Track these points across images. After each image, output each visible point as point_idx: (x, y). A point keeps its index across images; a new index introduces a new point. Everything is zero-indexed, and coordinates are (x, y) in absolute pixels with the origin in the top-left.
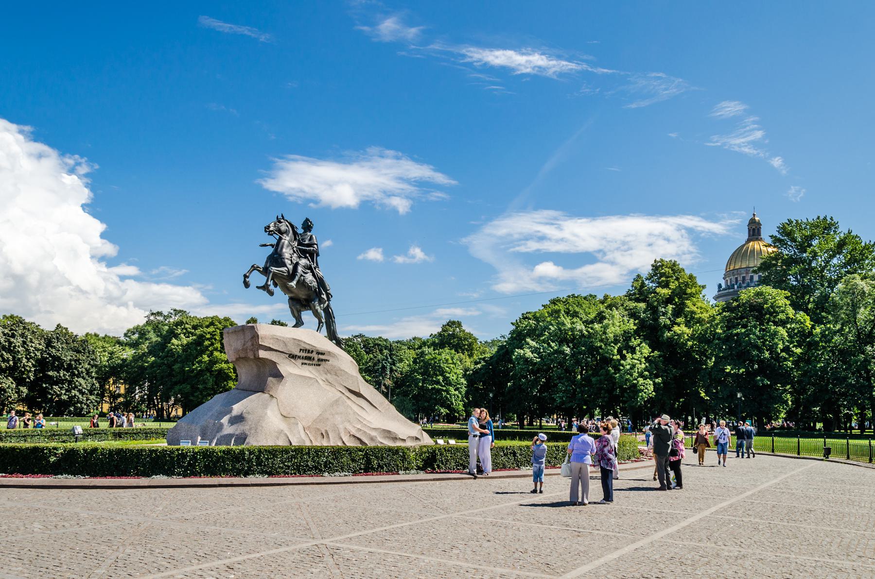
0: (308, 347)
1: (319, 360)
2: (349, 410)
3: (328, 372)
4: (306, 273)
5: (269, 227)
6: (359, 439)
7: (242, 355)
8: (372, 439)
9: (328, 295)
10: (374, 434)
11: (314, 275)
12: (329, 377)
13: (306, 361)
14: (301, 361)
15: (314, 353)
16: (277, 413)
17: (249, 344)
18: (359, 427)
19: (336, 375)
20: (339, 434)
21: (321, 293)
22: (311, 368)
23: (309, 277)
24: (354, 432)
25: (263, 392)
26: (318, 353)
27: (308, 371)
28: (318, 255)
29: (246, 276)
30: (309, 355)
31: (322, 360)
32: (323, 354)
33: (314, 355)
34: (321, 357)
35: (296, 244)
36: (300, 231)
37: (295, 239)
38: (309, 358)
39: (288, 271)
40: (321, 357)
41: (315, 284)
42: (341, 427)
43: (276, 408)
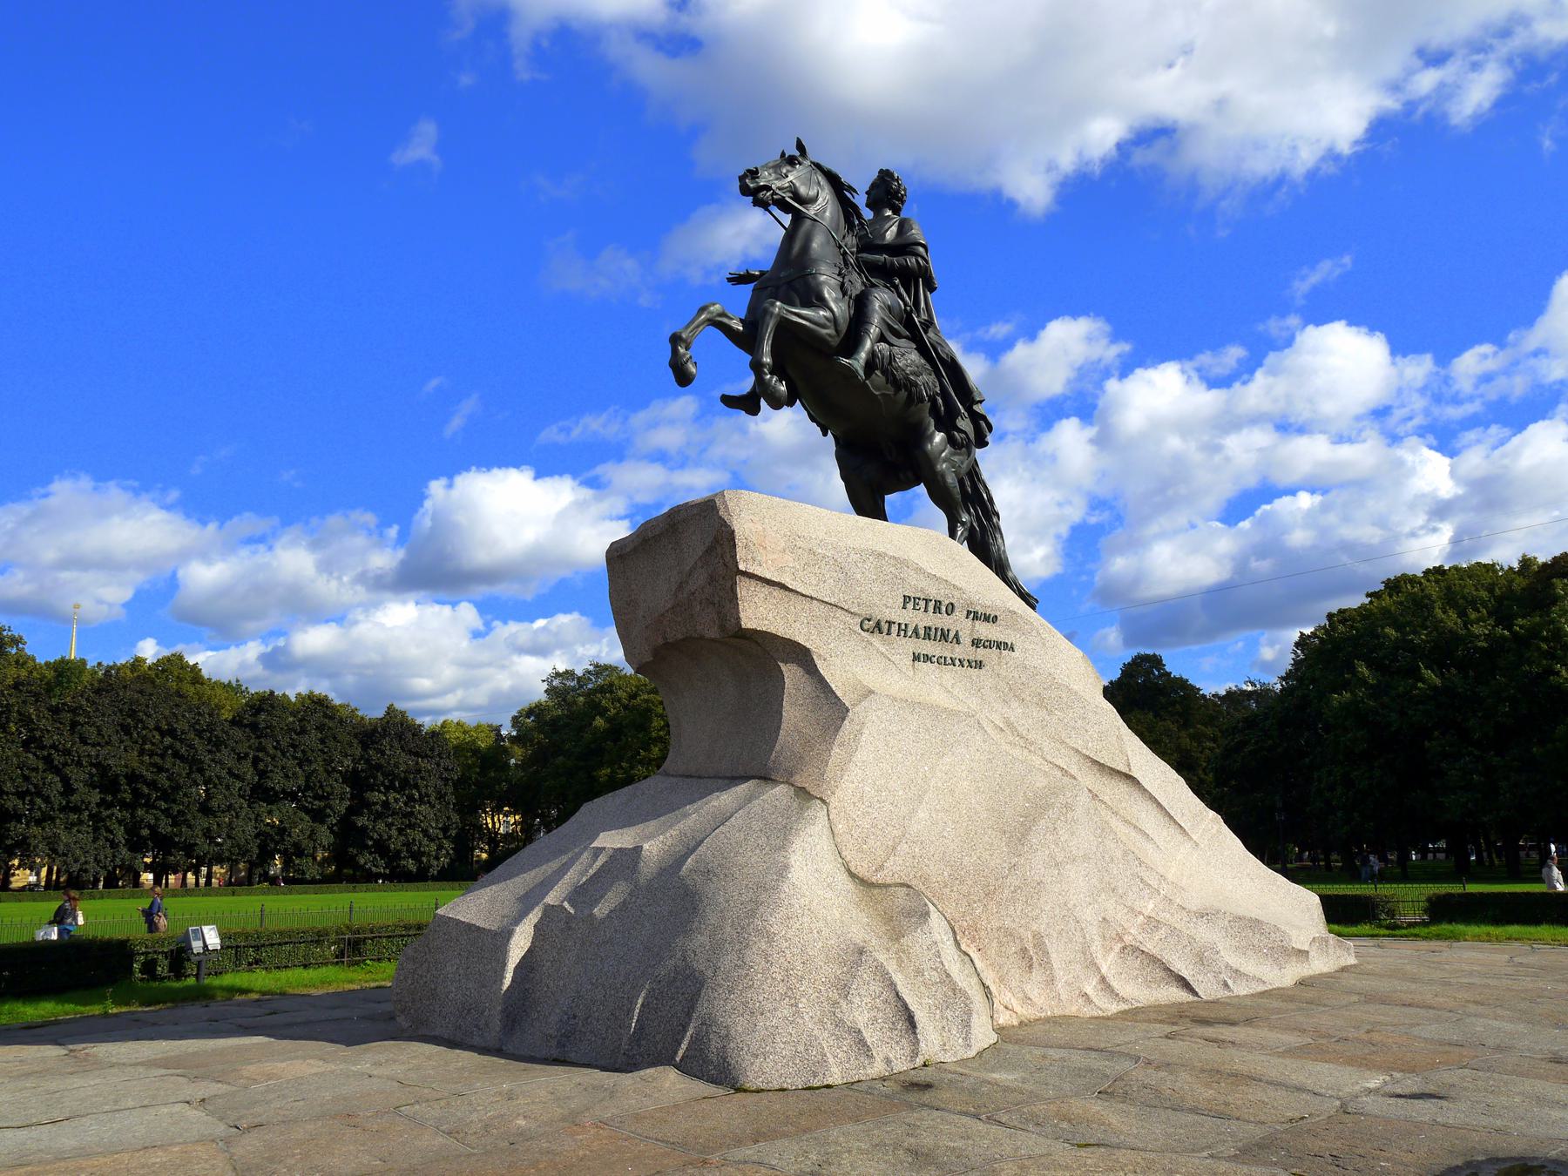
0: (934, 592)
1: (976, 643)
2: (1110, 844)
3: (1013, 693)
4: (898, 335)
5: (754, 174)
6: (1154, 960)
7: (676, 634)
8: (1202, 958)
9: (977, 418)
10: (1205, 934)
11: (923, 349)
12: (1015, 711)
13: (928, 647)
15: (959, 614)
16: (830, 866)
17: (700, 578)
18: (1149, 907)
19: (1041, 703)
20: (1085, 950)
21: (952, 414)
22: (949, 675)
23: (908, 358)
24: (1134, 934)
25: (766, 778)
26: (975, 616)
28: (930, 287)
29: (675, 340)
30: (941, 621)
31: (989, 644)
32: (990, 619)
33: (957, 622)
34: (984, 631)
35: (851, 241)
37: (851, 226)
38: (944, 636)
39: (835, 320)
40: (984, 631)
41: (927, 381)
42: (1089, 915)
43: (824, 844)
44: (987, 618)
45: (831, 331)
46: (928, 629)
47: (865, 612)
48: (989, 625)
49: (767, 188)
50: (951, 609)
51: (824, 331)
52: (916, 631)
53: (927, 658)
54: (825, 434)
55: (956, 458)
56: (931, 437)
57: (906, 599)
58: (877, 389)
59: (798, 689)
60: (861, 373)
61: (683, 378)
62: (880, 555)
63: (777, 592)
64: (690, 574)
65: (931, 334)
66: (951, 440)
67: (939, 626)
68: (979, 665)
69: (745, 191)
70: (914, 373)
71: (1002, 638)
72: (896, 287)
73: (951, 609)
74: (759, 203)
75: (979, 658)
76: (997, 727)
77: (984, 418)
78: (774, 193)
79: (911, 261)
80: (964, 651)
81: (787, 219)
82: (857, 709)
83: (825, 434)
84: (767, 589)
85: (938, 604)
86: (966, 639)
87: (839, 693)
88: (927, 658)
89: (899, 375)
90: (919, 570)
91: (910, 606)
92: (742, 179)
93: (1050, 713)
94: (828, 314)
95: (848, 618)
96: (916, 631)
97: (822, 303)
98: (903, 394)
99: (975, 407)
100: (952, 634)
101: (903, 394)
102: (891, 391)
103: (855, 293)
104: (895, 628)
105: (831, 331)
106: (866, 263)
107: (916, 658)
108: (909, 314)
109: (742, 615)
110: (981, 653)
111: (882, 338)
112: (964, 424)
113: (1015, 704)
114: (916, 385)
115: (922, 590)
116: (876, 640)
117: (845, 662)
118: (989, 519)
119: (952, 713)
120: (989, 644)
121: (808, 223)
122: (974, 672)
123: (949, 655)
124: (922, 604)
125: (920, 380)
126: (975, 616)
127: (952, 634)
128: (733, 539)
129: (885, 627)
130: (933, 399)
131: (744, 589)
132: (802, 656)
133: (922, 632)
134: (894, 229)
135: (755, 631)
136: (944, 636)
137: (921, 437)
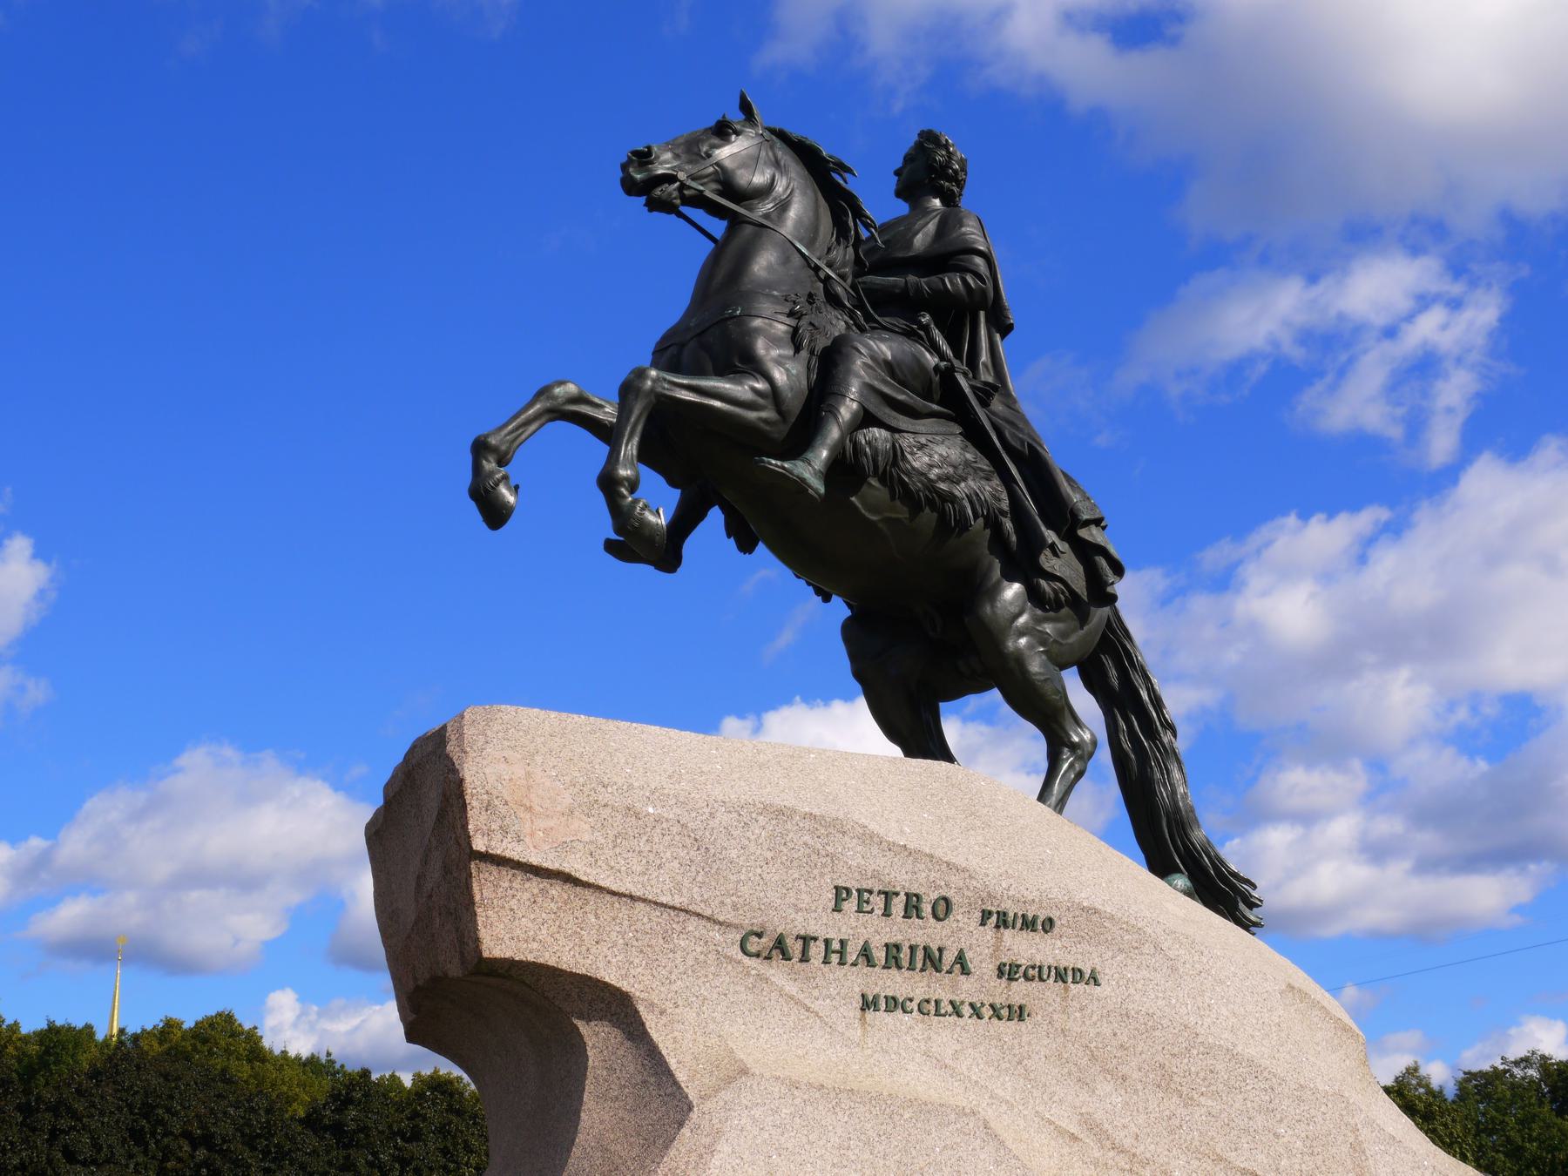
0: (902, 878)
1: (1008, 972)
5: (643, 157)
9: (1087, 553)
12: (1107, 1100)
14: (858, 980)
19: (1165, 1081)
22: (946, 1035)
26: (1003, 921)
27: (920, 1059)
30: (924, 932)
31: (1036, 973)
33: (961, 933)
34: (1023, 947)
35: (844, 254)
36: (880, 202)
38: (932, 960)
39: (775, 394)
40: (1023, 947)
44: (1029, 924)
45: (768, 414)
46: (893, 950)
47: (749, 921)
48: (1037, 937)
49: (670, 179)
50: (943, 909)
51: (752, 415)
52: (866, 954)
53: (893, 1004)
54: (827, 598)
55: (1048, 628)
56: (995, 591)
57: (841, 894)
58: (874, 509)
59: (611, 1069)
60: (818, 486)
61: (495, 514)
62: (781, 813)
63: (556, 889)
64: (425, 861)
65: (997, 405)
66: (1034, 595)
67: (920, 939)
68: (1019, 1013)
69: (630, 187)
70: (946, 478)
71: (1067, 961)
72: (926, 328)
73: (943, 909)
74: (655, 205)
75: (1017, 1000)
76: (1060, 1131)
77: (1103, 551)
78: (683, 186)
79: (952, 282)
80: (981, 986)
81: (718, 227)
82: (708, 1105)
83: (827, 598)
84: (535, 885)
85: (913, 906)
86: (983, 965)
87: (681, 1077)
88: (893, 1004)
89: (915, 484)
90: (868, 838)
91: (850, 905)
92: (624, 167)
93: (1188, 1102)
94: (760, 385)
95: (716, 935)
96: (866, 954)
97: (751, 365)
98: (928, 517)
99: (1082, 533)
100: (949, 958)
101: (928, 517)
102: (902, 513)
103: (822, 343)
104: (817, 950)
105: (768, 414)
106: (871, 292)
107: (868, 1004)
108: (947, 375)
109: (483, 933)
110: (1020, 991)
111: (866, 419)
112: (1063, 565)
113: (1105, 1087)
114: (953, 499)
115: (876, 875)
116: (777, 972)
117: (700, 1014)
118: (1152, 735)
119: (925, 1109)
120: (1036, 973)
121: (748, 230)
122: (1007, 1028)
123: (945, 997)
124: (878, 902)
125: (961, 490)
126: (1003, 921)
127: (949, 958)
128: (461, 795)
129: (795, 948)
130: (993, 522)
131: (487, 886)
132: (616, 1006)
133: (879, 955)
134: (932, 227)
135: (511, 964)
136: (932, 960)
137: (977, 590)
